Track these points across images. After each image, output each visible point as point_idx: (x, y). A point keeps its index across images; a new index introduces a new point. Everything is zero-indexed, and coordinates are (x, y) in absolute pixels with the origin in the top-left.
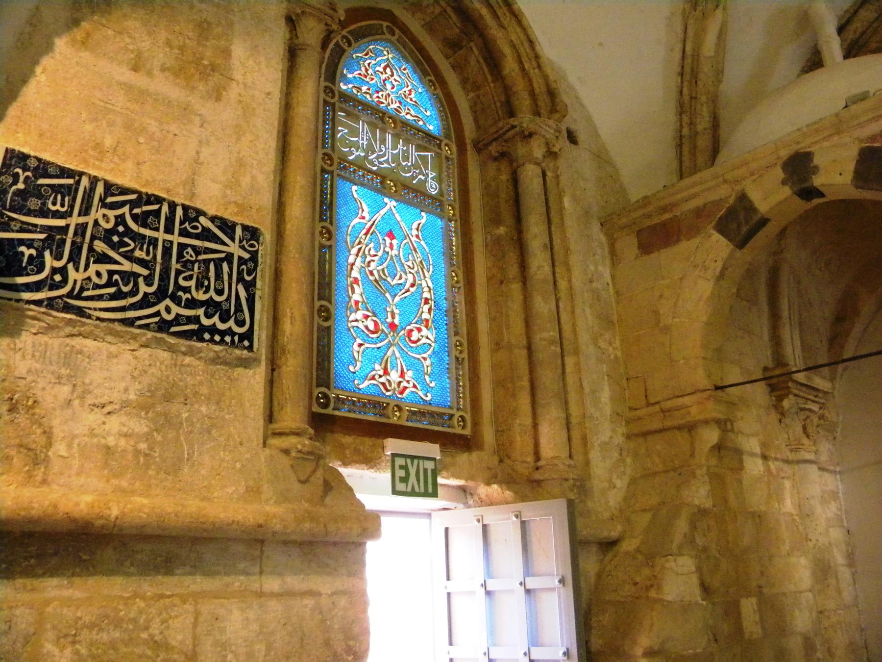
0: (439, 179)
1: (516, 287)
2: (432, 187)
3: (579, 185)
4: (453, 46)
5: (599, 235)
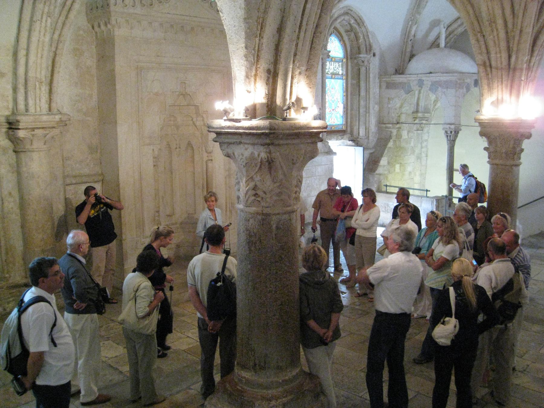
0: (342, 70)
1: (358, 96)
2: (340, 73)
3: (374, 65)
4: (347, 31)
5: (377, 80)
